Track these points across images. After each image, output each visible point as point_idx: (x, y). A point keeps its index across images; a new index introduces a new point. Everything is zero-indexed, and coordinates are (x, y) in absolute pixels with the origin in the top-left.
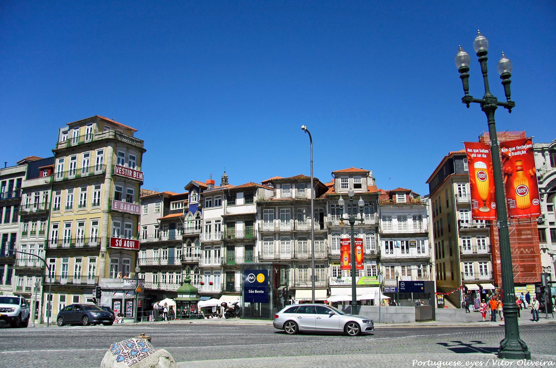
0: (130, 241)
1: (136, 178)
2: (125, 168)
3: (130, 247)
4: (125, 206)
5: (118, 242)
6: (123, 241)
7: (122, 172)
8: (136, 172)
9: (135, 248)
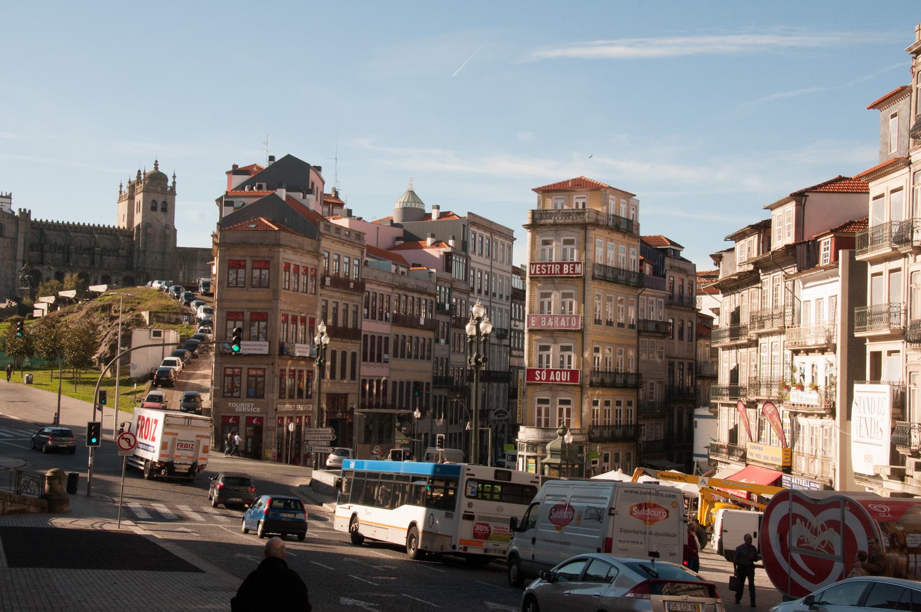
0: (561, 371)
1: (568, 273)
2: (546, 264)
3: (561, 380)
4: (550, 320)
5: (540, 375)
6: (548, 372)
7: (541, 270)
8: (569, 264)
9: (571, 381)
